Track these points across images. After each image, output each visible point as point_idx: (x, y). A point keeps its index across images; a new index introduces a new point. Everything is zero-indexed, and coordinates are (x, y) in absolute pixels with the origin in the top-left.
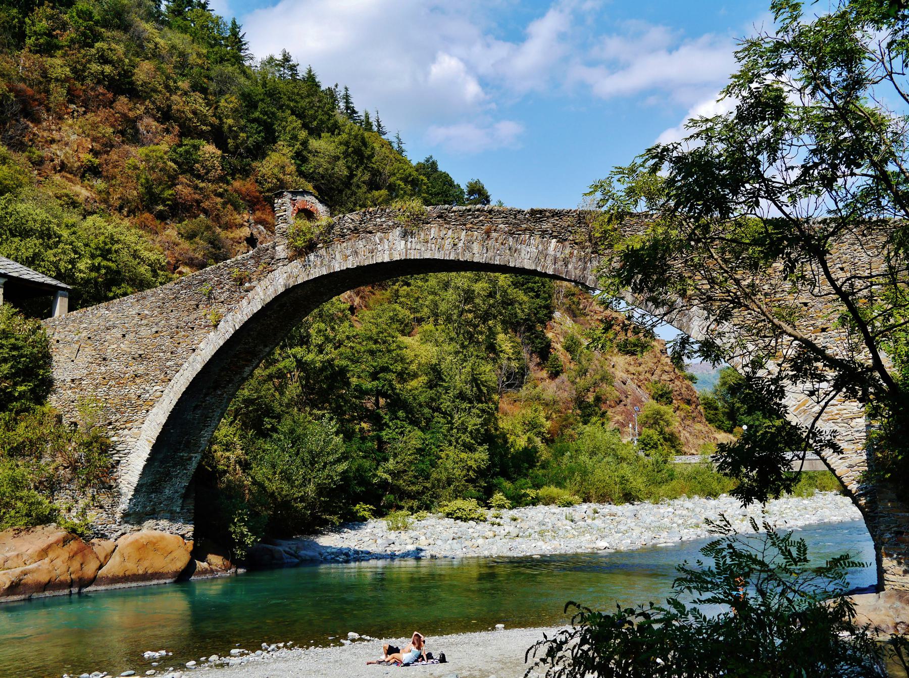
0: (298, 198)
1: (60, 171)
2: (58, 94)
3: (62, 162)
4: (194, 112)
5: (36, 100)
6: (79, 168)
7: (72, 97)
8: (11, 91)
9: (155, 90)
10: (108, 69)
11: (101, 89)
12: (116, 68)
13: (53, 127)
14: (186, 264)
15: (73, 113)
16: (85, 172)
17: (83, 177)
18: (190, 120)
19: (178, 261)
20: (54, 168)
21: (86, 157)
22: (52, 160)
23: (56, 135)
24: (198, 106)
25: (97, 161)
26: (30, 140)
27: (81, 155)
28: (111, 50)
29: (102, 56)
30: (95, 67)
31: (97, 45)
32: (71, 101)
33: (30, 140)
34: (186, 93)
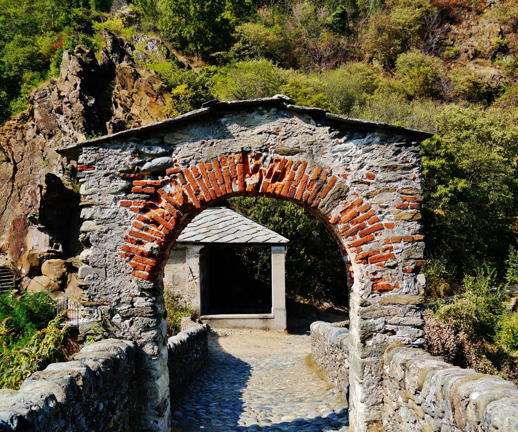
1: (472, 59)
3: (476, 51)
5: (459, 6)
6: (490, 52)
8: (434, 6)
13: (472, 23)
15: (490, 6)
16: (496, 53)
17: (494, 57)
20: (469, 57)
21: (495, 40)
22: (466, 52)
23: (474, 29)
25: (505, 41)
26: (452, 40)
27: (492, 40)
33: (452, 40)
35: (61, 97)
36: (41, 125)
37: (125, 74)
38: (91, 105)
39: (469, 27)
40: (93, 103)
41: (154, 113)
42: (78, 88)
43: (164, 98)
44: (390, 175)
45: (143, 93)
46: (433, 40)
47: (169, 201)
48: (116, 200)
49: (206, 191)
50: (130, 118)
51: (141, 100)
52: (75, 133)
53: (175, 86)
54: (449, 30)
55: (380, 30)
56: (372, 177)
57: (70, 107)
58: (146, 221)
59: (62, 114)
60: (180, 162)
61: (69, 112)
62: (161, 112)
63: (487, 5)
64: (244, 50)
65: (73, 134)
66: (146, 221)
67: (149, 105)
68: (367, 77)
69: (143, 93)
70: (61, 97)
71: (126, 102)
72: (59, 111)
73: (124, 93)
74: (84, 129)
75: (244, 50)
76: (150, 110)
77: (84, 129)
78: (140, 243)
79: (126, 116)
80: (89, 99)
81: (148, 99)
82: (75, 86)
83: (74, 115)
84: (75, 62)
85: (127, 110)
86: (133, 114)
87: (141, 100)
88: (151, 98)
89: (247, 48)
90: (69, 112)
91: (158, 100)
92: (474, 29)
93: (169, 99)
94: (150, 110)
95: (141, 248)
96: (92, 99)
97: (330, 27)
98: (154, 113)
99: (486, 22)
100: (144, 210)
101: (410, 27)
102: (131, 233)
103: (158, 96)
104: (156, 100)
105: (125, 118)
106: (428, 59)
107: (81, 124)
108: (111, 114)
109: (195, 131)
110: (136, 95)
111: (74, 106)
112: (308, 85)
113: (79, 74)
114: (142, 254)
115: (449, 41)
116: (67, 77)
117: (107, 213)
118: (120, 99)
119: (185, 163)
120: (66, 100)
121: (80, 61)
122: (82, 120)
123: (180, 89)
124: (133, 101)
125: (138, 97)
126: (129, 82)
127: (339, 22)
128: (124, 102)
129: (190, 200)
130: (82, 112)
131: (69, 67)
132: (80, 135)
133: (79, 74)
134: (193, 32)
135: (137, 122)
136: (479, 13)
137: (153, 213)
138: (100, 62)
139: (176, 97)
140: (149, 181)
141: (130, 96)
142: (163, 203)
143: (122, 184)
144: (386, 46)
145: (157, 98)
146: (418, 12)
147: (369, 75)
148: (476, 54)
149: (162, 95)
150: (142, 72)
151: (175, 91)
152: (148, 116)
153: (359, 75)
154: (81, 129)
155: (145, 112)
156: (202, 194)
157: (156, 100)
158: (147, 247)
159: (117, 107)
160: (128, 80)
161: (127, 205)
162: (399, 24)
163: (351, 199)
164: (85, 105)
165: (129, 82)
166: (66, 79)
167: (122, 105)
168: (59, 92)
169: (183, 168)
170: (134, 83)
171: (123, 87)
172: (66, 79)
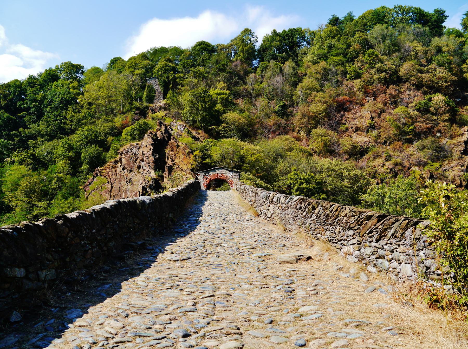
0: (210, 173)
1: (355, 132)
2: (360, 95)
3: (357, 127)
4: (440, 78)
6: (366, 128)
7: (366, 94)
9: (411, 76)
10: (382, 75)
11: (379, 86)
12: (388, 73)
13: (357, 111)
14: (416, 165)
16: (368, 129)
17: (367, 131)
18: (437, 83)
19: (410, 164)
20: (353, 131)
21: (368, 122)
22: (352, 128)
24: (441, 75)
28: (385, 65)
29: (380, 70)
30: (376, 77)
31: (377, 66)
32: (367, 96)
34: (435, 70)
35: (143, 154)
36: (127, 166)
39: (355, 113)
42: (152, 150)
45: (181, 154)
46: (333, 122)
50: (174, 164)
52: (150, 170)
53: (195, 151)
54: (344, 115)
55: (304, 115)
57: (148, 159)
59: (143, 161)
61: (147, 161)
62: (188, 162)
63: (367, 101)
64: (226, 127)
69: (181, 154)
70: (143, 154)
72: (142, 160)
73: (172, 153)
75: (226, 127)
81: (183, 157)
82: (150, 149)
84: (150, 139)
85: (173, 160)
89: (228, 127)
90: (147, 161)
92: (358, 115)
93: (192, 157)
97: (276, 112)
99: (365, 111)
101: (320, 114)
106: (330, 132)
107: (153, 166)
108: (166, 163)
112: (255, 150)
113: (152, 145)
115: (343, 121)
120: (146, 155)
121: (153, 139)
123: (196, 153)
127: (282, 110)
131: (148, 141)
133: (152, 145)
134: (200, 118)
136: (363, 105)
138: (159, 138)
139: (195, 156)
141: (175, 155)
144: (308, 123)
146: (324, 106)
148: (358, 129)
150: (180, 144)
151: (194, 154)
159: (168, 159)
162: (313, 112)
164: (155, 158)
166: (146, 146)
167: (171, 159)
168: (143, 152)
171: (172, 151)
172: (146, 146)
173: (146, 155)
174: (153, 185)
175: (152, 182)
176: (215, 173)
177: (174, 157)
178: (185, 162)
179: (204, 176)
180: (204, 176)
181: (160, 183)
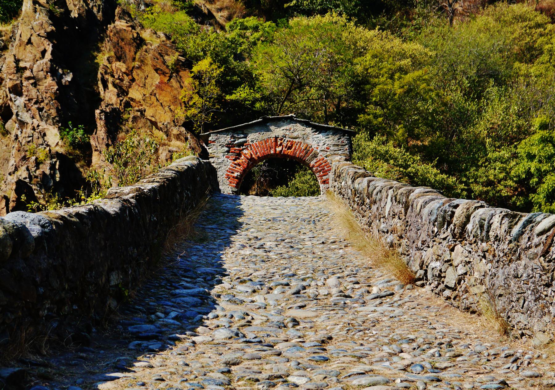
35: (20, 70)
37: (123, 40)
38: (67, 83)
40: (69, 80)
41: (165, 99)
42: (48, 56)
43: (181, 77)
44: (336, 148)
45: (148, 69)
47: (245, 157)
48: (223, 155)
49: (260, 153)
50: (128, 105)
51: (145, 79)
52: (43, 125)
53: (198, 59)
56: (328, 149)
57: (35, 85)
58: (235, 164)
59: (20, 94)
60: (250, 141)
61: (33, 93)
62: (175, 98)
65: (38, 126)
66: (235, 164)
67: (158, 87)
68: (534, 31)
69: (148, 69)
70: (20, 70)
71: (122, 80)
72: (17, 90)
73: (120, 66)
74: (57, 118)
76: (160, 94)
77: (57, 118)
78: (233, 173)
79: (121, 101)
80: (64, 74)
81: (157, 79)
82: (44, 53)
83: (40, 97)
84: (42, 17)
85: (122, 92)
86: (132, 99)
87: (145, 79)
88: (162, 76)
90: (33, 93)
91: (172, 80)
93: (188, 80)
94: (160, 94)
95: (233, 175)
96: (68, 73)
98: (165, 99)
100: (235, 160)
102: (229, 169)
103: (172, 73)
104: (169, 80)
105: (121, 105)
107: (53, 112)
108: (97, 100)
109: (256, 128)
110: (139, 71)
111: (40, 83)
112: (403, 56)
113: (49, 36)
114: (233, 177)
116: (29, 40)
117: (220, 161)
118: (113, 76)
119: (252, 141)
120: (28, 73)
121: (51, 15)
122: (56, 105)
123: (203, 65)
124: (133, 80)
125: (141, 74)
126: (129, 51)
128: (118, 81)
129: (254, 156)
130: (55, 93)
131: (34, 24)
132: (51, 128)
133: (49, 36)
135: (138, 111)
137: (238, 161)
138: (74, 14)
139: (198, 77)
140: (237, 148)
141: (130, 72)
142: (243, 157)
143: (226, 149)
145: (171, 77)
147: (538, 26)
149: (177, 72)
150: (146, 35)
151: (195, 69)
152: (156, 103)
153: (518, 28)
154: (53, 118)
155: (153, 97)
156: (258, 154)
157: (169, 80)
158: (236, 174)
159: (105, 87)
160: (127, 49)
161: (228, 158)
163: (319, 157)
164: (59, 83)
165: (129, 51)
166: (29, 42)
167: (115, 85)
168: (17, 61)
169: (251, 143)
170: (135, 53)
171: (119, 59)
172: (29, 42)
173: (28, 73)
174: (53, 176)
175: (52, 167)
176: (265, 135)
177: (126, 79)
178: (165, 98)
179: (229, 146)
180: (229, 145)
181: (77, 170)
